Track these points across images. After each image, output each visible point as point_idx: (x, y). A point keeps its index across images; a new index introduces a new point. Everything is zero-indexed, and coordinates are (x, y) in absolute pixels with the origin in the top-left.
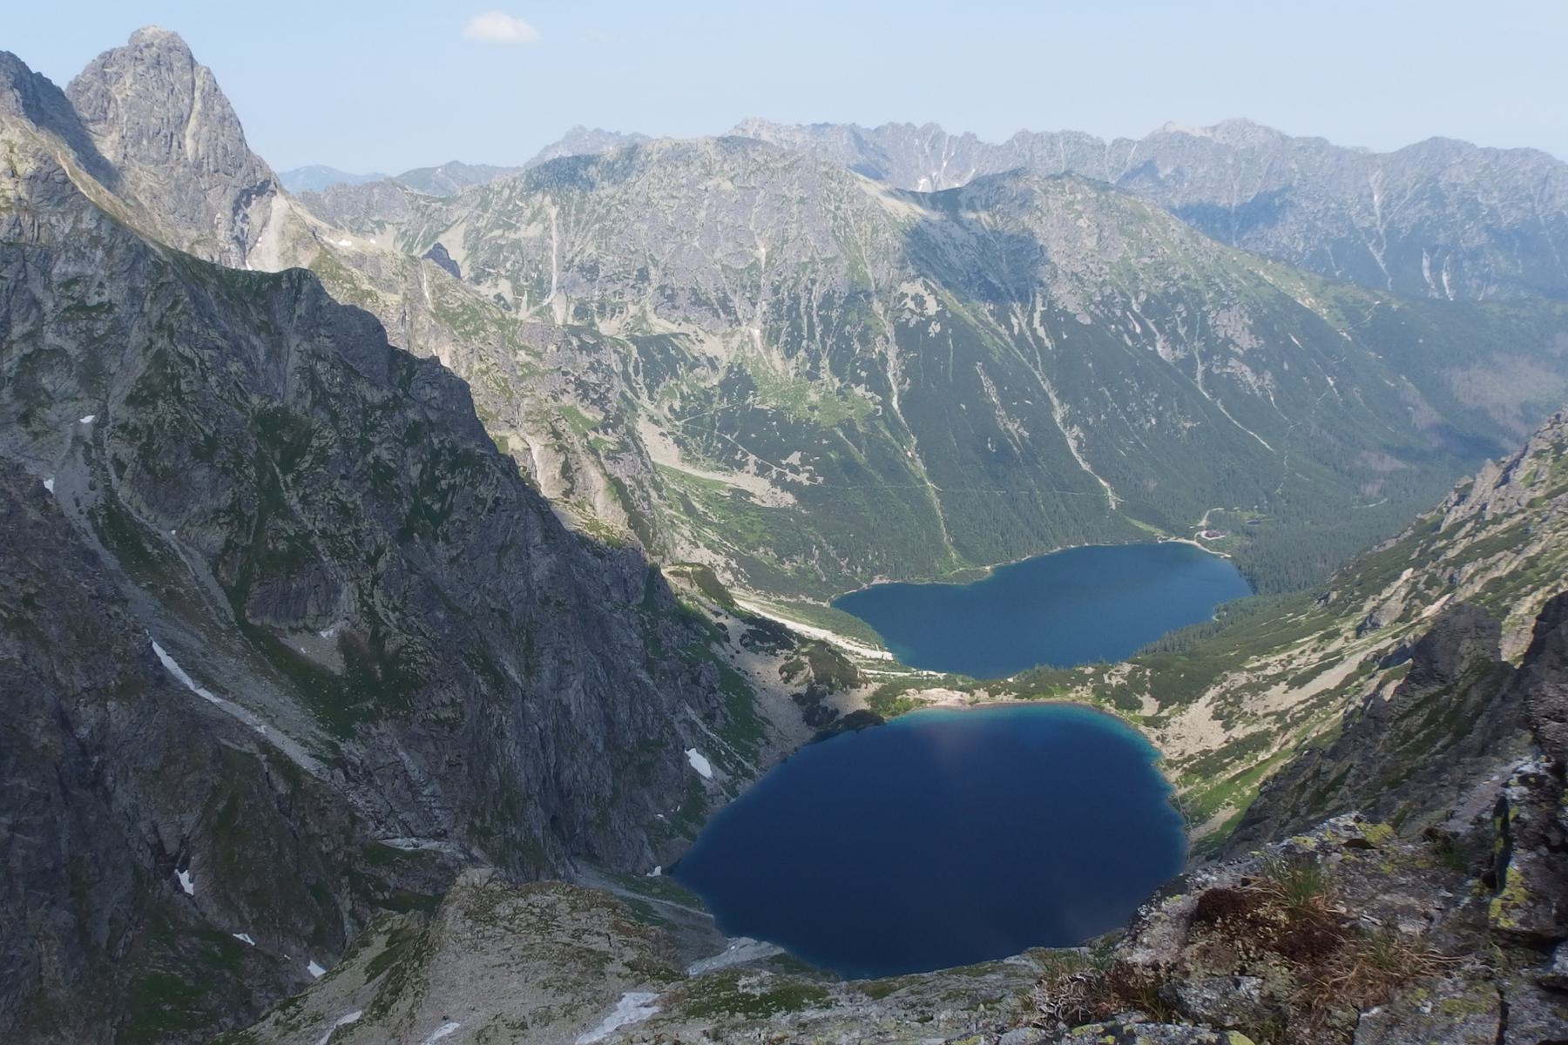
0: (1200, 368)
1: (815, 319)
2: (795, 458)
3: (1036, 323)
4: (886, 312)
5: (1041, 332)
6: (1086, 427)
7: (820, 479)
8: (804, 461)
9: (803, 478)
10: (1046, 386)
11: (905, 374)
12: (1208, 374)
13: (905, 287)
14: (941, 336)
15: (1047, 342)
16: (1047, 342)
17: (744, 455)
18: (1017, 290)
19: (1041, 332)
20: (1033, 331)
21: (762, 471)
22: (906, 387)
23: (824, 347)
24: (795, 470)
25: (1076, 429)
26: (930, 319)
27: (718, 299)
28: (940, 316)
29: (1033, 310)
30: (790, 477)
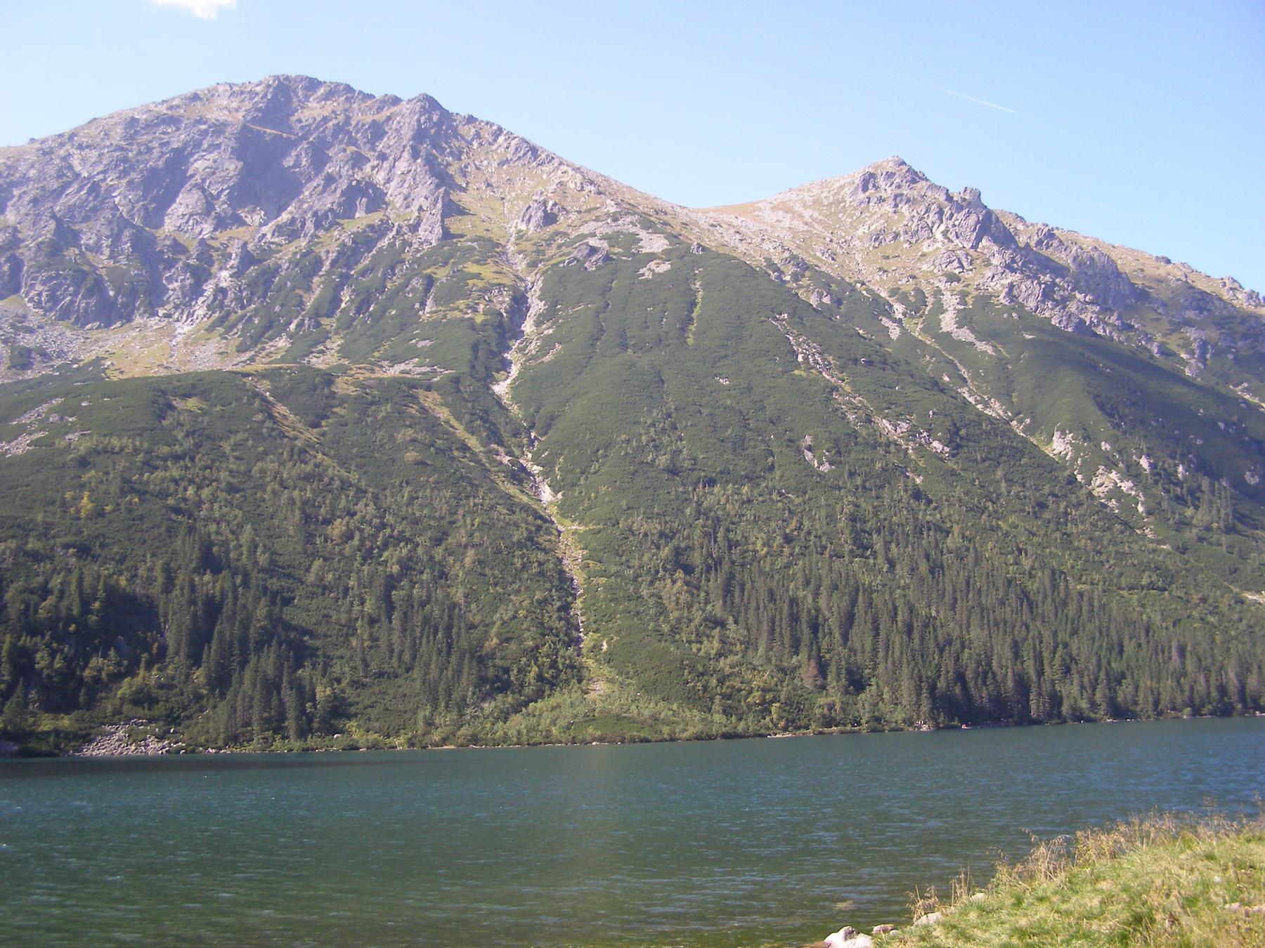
3: (948, 322)
4: (533, 265)
5: (965, 335)
6: (1132, 472)
14: (679, 281)
16: (982, 346)
18: (893, 292)
19: (965, 335)
26: (652, 257)
28: (667, 255)
29: (939, 309)
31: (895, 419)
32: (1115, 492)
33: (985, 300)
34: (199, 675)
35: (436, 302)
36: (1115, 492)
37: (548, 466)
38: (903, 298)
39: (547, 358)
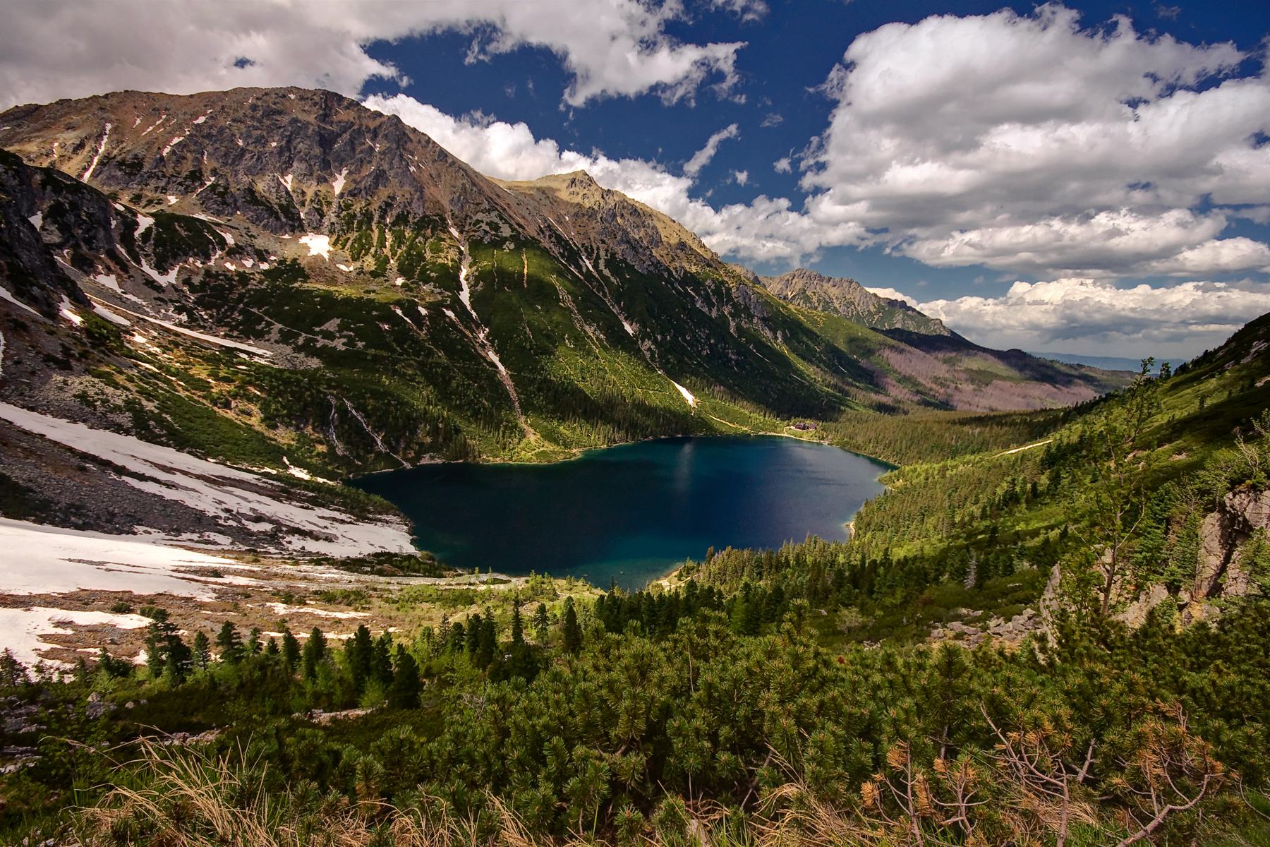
0: (733, 324)
1: (388, 236)
2: (332, 325)
3: (602, 266)
5: (607, 272)
6: (655, 342)
7: (360, 344)
8: (342, 328)
9: (339, 344)
10: (615, 310)
11: (477, 279)
12: (739, 328)
13: (480, 216)
15: (612, 279)
16: (612, 279)
17: (269, 324)
19: (607, 272)
20: (600, 272)
21: (285, 338)
22: (479, 288)
23: (394, 255)
24: (329, 335)
25: (648, 343)
26: (505, 240)
27: (281, 206)
29: (598, 257)
30: (321, 342)
31: (590, 325)
32: (649, 349)
33: (613, 255)
34: (441, 440)
35: (431, 250)
36: (649, 349)
37: (492, 342)
38: (586, 250)
39: (479, 288)
